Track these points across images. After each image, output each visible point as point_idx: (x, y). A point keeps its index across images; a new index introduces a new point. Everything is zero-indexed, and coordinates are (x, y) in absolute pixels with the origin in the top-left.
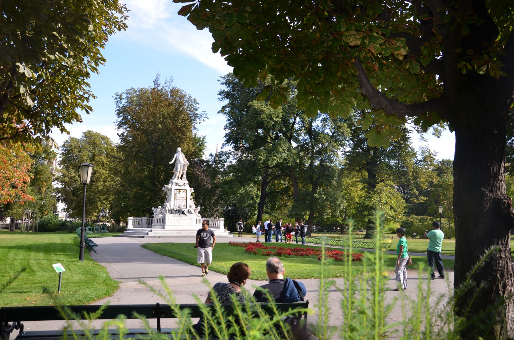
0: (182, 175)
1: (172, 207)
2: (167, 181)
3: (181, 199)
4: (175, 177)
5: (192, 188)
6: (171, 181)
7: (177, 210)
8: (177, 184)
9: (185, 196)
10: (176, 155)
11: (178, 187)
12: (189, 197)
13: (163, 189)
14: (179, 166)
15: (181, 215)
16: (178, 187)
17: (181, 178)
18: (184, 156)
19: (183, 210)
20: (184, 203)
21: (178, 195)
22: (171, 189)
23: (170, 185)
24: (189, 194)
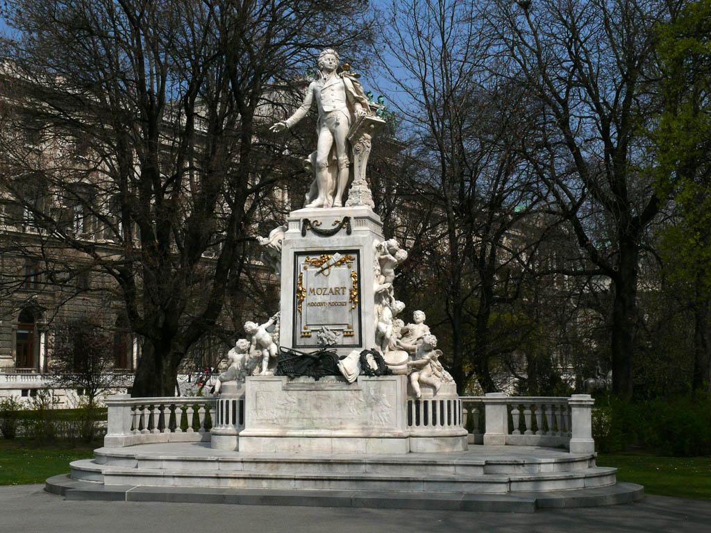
0: (349, 186)
1: (286, 343)
3: (327, 299)
4: (315, 196)
7: (305, 356)
8: (307, 225)
9: (349, 284)
11: (315, 242)
12: (375, 282)
14: (325, 138)
16: (315, 242)
17: (345, 198)
19: (340, 352)
21: (310, 277)
22: (280, 253)
23: (275, 236)
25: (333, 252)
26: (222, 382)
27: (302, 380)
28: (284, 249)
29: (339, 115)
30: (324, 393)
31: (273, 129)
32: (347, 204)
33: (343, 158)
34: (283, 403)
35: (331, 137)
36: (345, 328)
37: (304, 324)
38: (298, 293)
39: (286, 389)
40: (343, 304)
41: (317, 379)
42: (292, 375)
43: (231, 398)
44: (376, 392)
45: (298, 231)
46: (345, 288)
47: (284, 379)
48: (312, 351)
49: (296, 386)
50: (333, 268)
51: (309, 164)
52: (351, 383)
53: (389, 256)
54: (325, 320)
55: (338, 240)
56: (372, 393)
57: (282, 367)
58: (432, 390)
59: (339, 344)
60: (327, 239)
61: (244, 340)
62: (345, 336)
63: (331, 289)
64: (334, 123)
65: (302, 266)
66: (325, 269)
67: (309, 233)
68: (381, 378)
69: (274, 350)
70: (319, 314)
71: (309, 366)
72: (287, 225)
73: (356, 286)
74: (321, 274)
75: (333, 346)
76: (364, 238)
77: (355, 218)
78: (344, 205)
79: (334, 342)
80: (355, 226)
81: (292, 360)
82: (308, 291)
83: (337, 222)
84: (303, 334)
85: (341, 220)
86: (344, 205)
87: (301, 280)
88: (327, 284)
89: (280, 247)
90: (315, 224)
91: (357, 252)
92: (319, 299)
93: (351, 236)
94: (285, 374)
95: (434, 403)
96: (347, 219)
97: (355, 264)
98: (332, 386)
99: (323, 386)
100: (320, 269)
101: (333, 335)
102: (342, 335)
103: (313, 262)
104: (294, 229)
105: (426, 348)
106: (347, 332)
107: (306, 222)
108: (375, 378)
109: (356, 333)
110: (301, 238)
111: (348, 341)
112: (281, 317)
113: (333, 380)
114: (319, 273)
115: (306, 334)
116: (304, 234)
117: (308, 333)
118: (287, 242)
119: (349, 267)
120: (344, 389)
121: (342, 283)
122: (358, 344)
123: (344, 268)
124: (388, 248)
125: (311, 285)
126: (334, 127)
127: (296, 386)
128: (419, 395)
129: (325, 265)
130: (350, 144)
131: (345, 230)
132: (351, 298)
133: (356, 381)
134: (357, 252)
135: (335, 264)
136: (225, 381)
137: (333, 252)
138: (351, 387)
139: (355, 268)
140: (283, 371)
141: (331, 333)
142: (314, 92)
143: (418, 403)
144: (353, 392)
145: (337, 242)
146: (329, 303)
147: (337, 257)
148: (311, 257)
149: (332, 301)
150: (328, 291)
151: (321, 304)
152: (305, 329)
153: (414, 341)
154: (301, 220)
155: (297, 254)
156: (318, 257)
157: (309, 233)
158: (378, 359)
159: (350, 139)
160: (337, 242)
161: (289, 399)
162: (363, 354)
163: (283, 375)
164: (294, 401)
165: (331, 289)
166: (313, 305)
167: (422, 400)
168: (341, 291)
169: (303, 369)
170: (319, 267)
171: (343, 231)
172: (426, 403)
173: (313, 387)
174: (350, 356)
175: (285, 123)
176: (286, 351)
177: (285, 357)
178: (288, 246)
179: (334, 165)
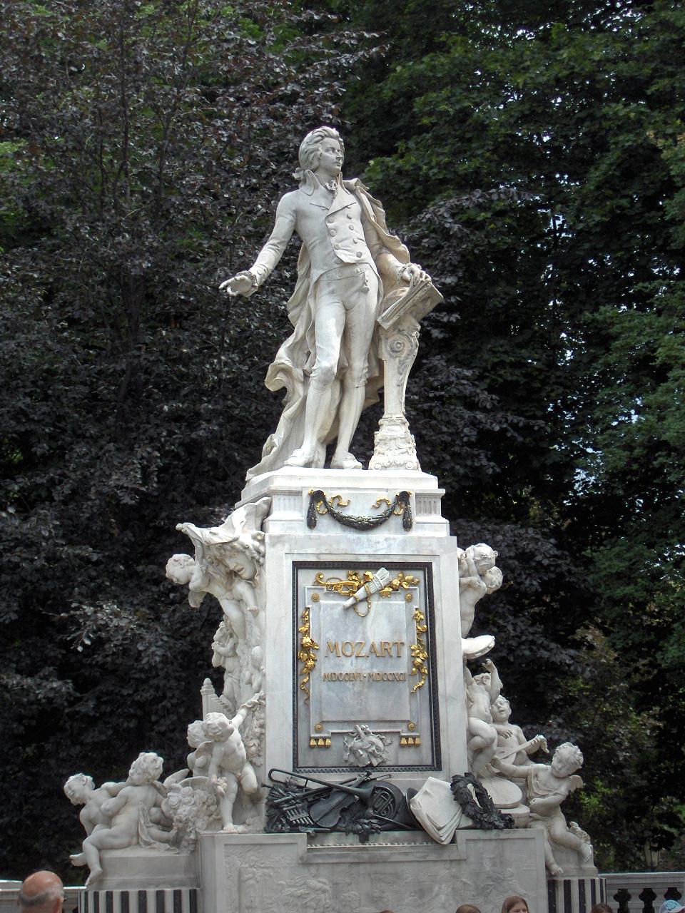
1: (278, 755)
2: (217, 489)
3: (365, 667)
5: (485, 550)
6: (254, 478)
7: (328, 790)
9: (409, 637)
10: (288, 201)
11: (333, 541)
13: (178, 567)
15: (385, 842)
16: (333, 541)
17: (363, 448)
18: (377, 212)
20: (409, 707)
22: (257, 561)
24: (452, 612)
25: (375, 566)
26: (99, 850)
27: (332, 841)
28: (270, 552)
29: (367, 273)
30: (388, 869)
31: (225, 288)
32: (375, 460)
33: (359, 365)
34: (299, 892)
35: (344, 317)
36: (403, 730)
37: (314, 720)
38: (302, 653)
39: (305, 863)
40: (396, 679)
41: (364, 837)
42: (310, 830)
43: (149, 884)
44: (494, 865)
45: (301, 515)
46: (402, 643)
47: (301, 838)
48: (343, 780)
49: (329, 856)
50: (376, 603)
51: (286, 371)
52: (445, 846)
53: (476, 578)
54: (360, 710)
55: (386, 540)
56: (488, 867)
57: (284, 814)
58: (573, 858)
59: (389, 763)
60: (363, 536)
61: (152, 755)
62: (402, 746)
63: (373, 646)
64: (355, 288)
65: (308, 595)
66: (361, 601)
67: (324, 522)
68: (505, 834)
69: (251, 777)
70: (349, 698)
71: (343, 810)
72: (270, 505)
73: (424, 639)
74: (352, 613)
75: (380, 767)
76: (439, 539)
77: (417, 495)
78: (366, 466)
79: (380, 760)
80: (419, 512)
81: (303, 799)
82: (323, 647)
83: (385, 501)
84: (313, 743)
85: (391, 498)
86: (366, 466)
87: (308, 621)
88: (364, 633)
89: (262, 549)
90: (335, 505)
91: (426, 568)
92: (348, 666)
93: (414, 533)
94: (294, 828)
95: (581, 883)
96: (404, 497)
97: (419, 593)
98: (407, 854)
99: (384, 852)
100: (350, 602)
101: (380, 744)
102: (396, 744)
103: (332, 586)
104: (287, 518)
105: (563, 772)
106: (407, 738)
107: (317, 496)
108: (493, 834)
109: (425, 741)
110: (307, 532)
111: (407, 757)
112: (268, 703)
113: (397, 841)
114: (347, 609)
115: (321, 742)
116: (311, 524)
117: (324, 739)
118: (278, 540)
119: (409, 600)
120: (428, 859)
121: (396, 632)
122: (429, 762)
123: (398, 603)
124: (476, 562)
125: (330, 635)
126: (353, 298)
127: (329, 856)
128: (556, 868)
129: (360, 593)
130: (377, 334)
131: (400, 520)
132: (414, 665)
133: (453, 841)
134: (426, 568)
135: (380, 593)
136: (113, 848)
137: (375, 566)
138: (445, 857)
139: (419, 601)
140: (290, 823)
141: (374, 739)
142: (298, 215)
143: (552, 884)
144: (448, 865)
145: (385, 545)
146: (370, 676)
147: (382, 576)
148: (327, 575)
149: (375, 671)
150: (365, 651)
151: (351, 677)
152: (318, 731)
153: (513, 758)
154: (305, 494)
155: (298, 566)
156: (342, 575)
157: (324, 522)
158: (482, 794)
159: (386, 326)
160: (385, 545)
161: (314, 883)
162: (457, 786)
163: (291, 831)
164: (327, 887)
165: (373, 646)
166: (333, 678)
167: (561, 879)
168: (393, 653)
169: (331, 822)
170: (348, 596)
171: (396, 522)
172: (567, 884)
173: (365, 856)
174: (425, 787)
175: (253, 278)
176: (281, 777)
177: (285, 791)
178: (282, 549)
179: (342, 376)
